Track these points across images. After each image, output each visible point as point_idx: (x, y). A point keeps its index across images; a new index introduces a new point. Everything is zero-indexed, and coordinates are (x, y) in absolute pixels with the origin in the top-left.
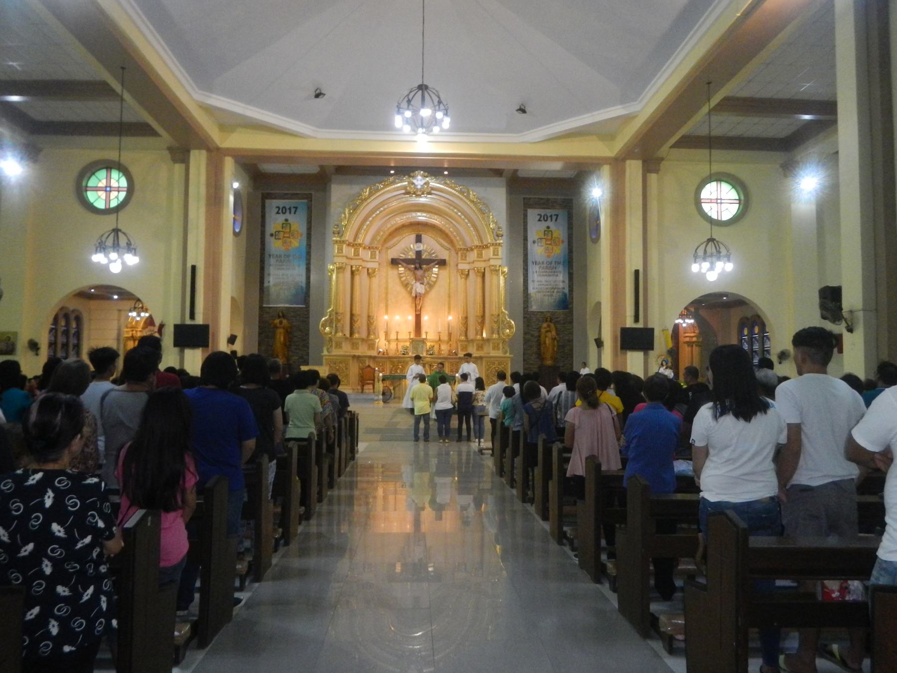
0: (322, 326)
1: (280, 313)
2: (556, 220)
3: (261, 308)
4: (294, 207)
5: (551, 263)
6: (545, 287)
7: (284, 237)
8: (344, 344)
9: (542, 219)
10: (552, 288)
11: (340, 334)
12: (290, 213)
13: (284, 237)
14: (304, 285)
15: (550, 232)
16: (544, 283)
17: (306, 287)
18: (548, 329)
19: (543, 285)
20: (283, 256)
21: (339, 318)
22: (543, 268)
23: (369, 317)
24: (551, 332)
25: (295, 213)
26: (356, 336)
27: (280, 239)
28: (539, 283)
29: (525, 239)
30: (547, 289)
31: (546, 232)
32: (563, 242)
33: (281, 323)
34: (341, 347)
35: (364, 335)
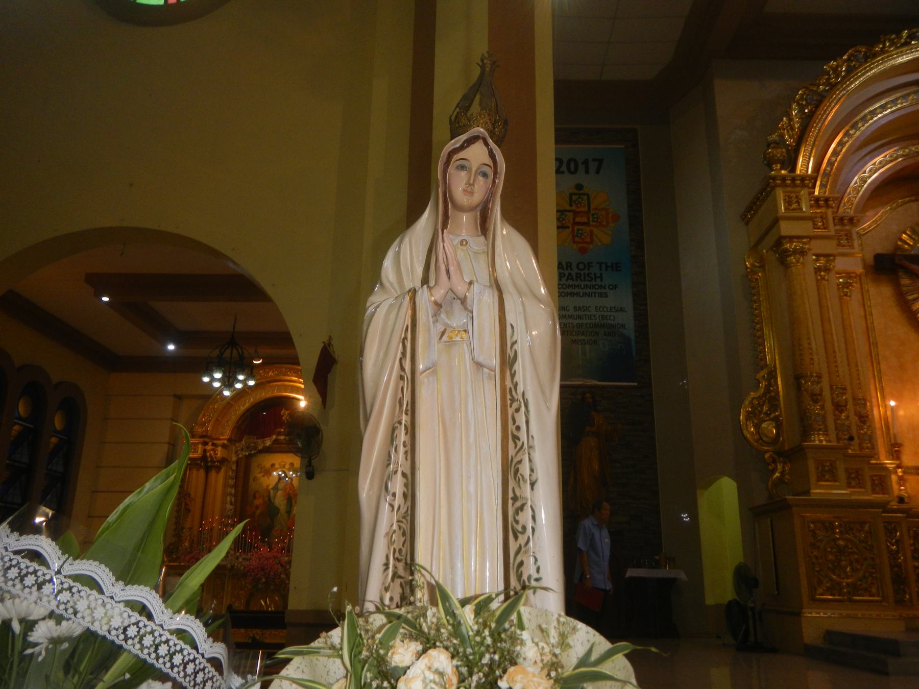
0: (749, 416)
1: (588, 395)
4: (594, 160)
7: (575, 223)
11: (818, 440)
12: (587, 172)
13: (576, 223)
14: (630, 331)
20: (574, 266)
25: (598, 172)
27: (568, 227)
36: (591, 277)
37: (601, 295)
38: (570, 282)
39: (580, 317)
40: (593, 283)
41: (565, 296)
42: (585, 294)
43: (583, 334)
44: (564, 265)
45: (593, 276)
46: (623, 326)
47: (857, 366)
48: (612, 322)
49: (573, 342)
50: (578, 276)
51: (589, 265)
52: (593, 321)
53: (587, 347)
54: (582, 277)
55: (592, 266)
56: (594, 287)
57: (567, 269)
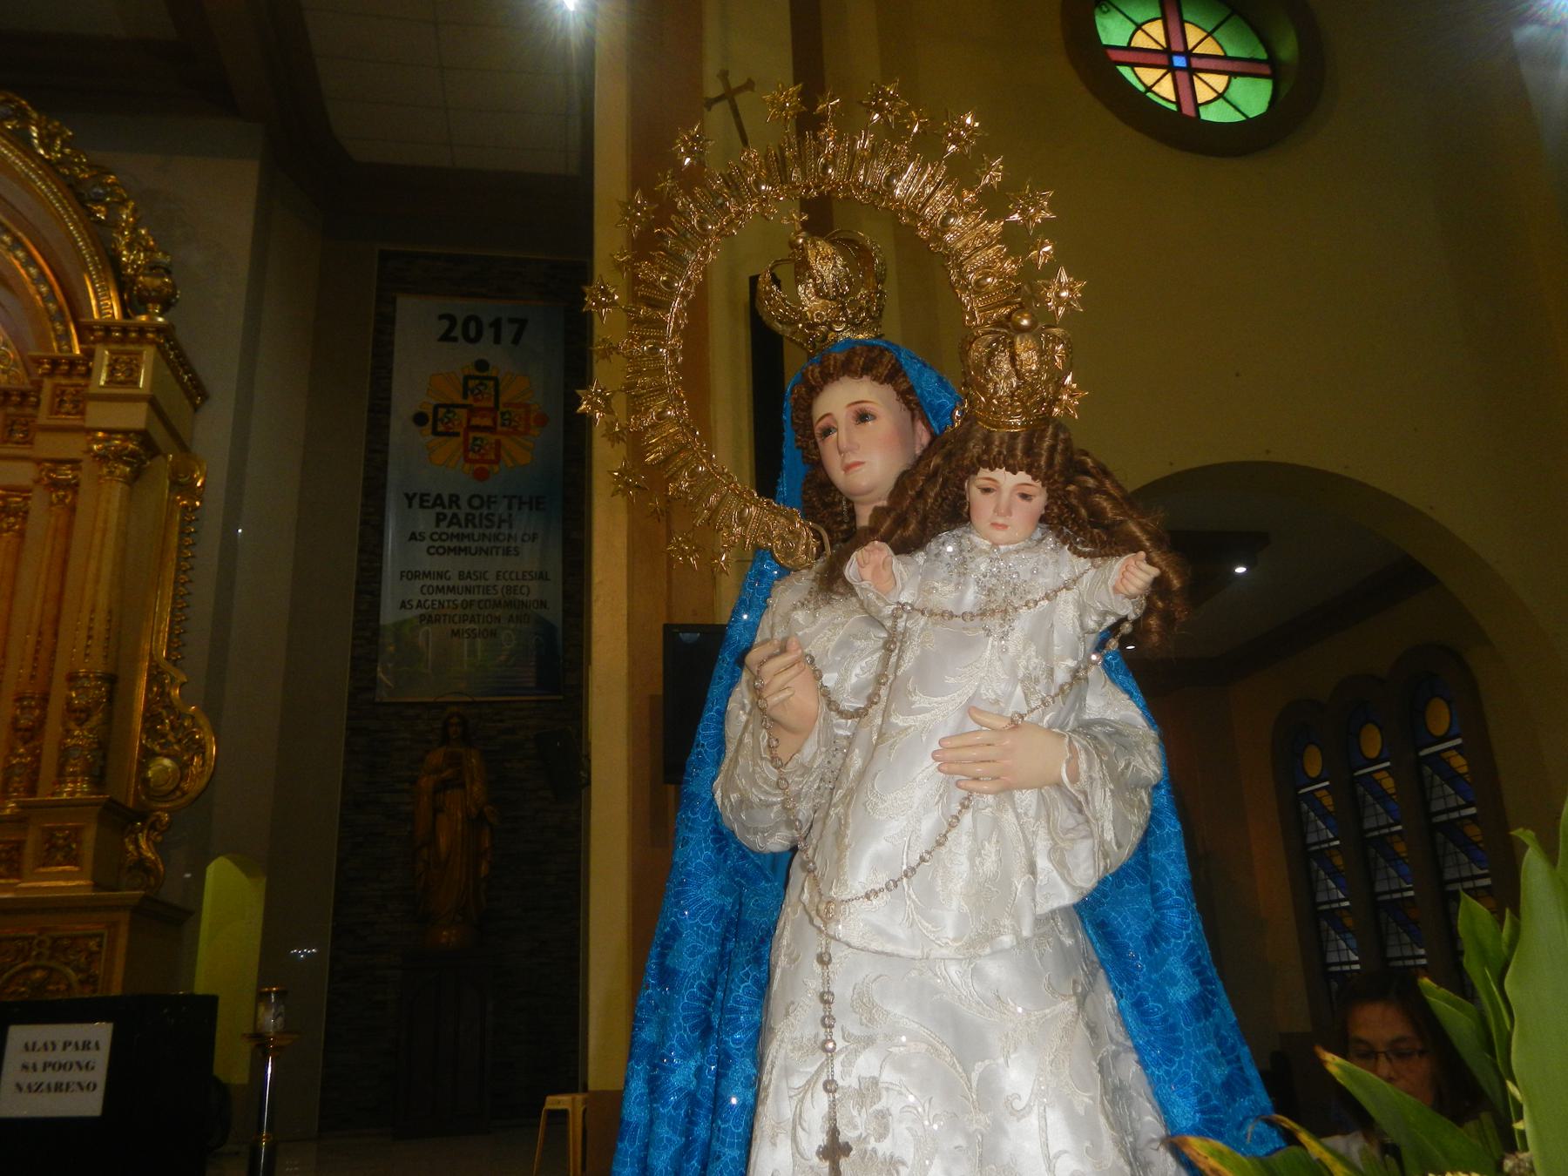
2: (516, 341)
5: (489, 501)
6: (460, 598)
9: (457, 332)
10: (497, 604)
15: (491, 384)
16: (455, 582)
18: (447, 773)
19: (452, 589)
22: (454, 520)
24: (463, 785)
28: (440, 583)
29: (380, 409)
30: (470, 604)
31: (472, 384)
32: (542, 421)
41: (444, 553)
55: (495, 502)
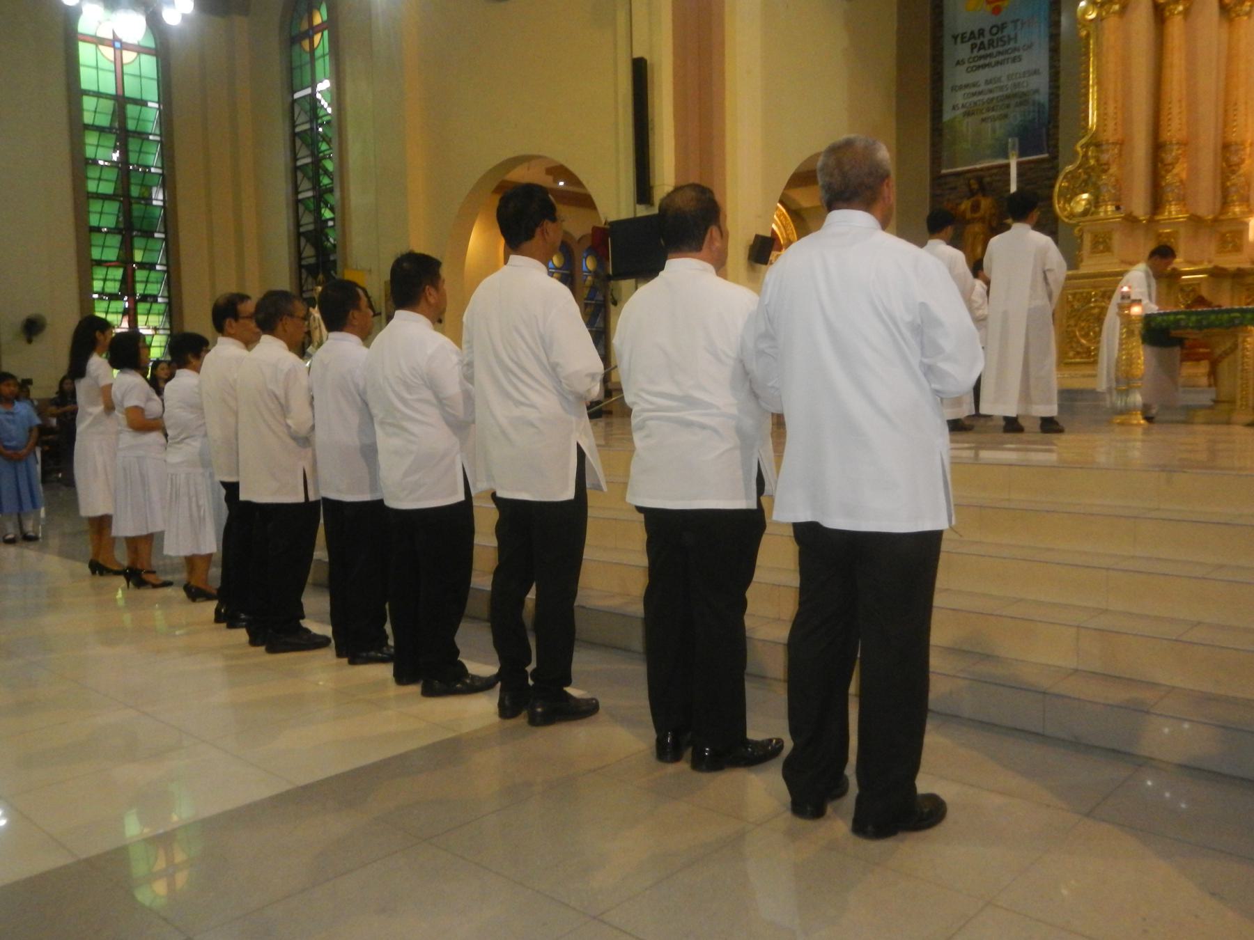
1: (972, 181)
3: (938, 180)
8: (1117, 239)
14: (1043, 97)
17: (1050, 101)
20: (987, 33)
21: (1105, 157)
23: (1226, 147)
26: (1173, 211)
33: (976, 207)
34: (1108, 249)
35: (1205, 207)
36: (1002, 41)
37: (1014, 60)
38: (982, 52)
39: (991, 91)
40: (1007, 47)
42: (998, 63)
43: (993, 109)
44: (976, 32)
45: (1006, 39)
46: (1037, 91)
47: (1236, 104)
48: (1024, 90)
49: (983, 120)
50: (991, 43)
51: (1002, 27)
52: (1005, 93)
53: (997, 124)
54: (995, 44)
56: (1006, 52)
57: (979, 37)
